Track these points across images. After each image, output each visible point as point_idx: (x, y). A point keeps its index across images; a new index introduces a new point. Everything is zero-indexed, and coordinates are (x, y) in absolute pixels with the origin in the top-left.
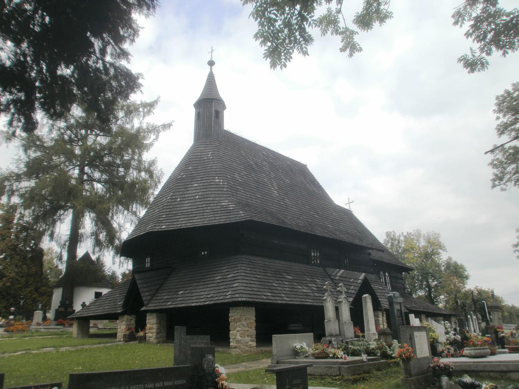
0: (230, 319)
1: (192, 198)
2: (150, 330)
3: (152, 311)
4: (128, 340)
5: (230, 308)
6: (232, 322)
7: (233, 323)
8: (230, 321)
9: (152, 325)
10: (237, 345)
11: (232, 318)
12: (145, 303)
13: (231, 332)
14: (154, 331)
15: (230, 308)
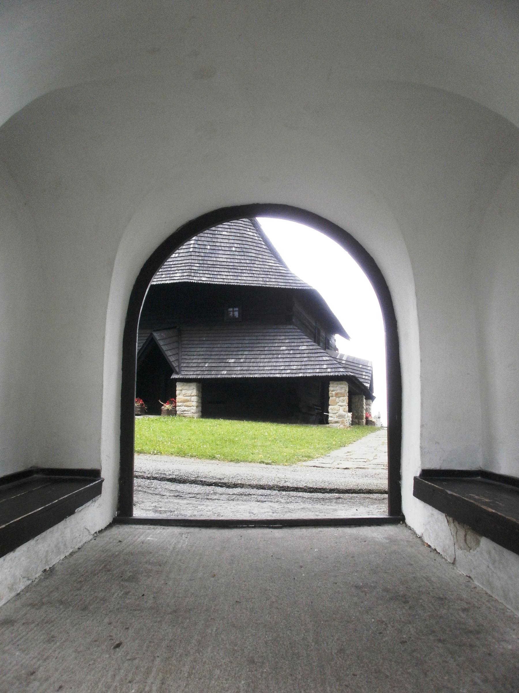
0: (331, 393)
1: (227, 249)
2: (184, 402)
3: (187, 381)
4: (139, 413)
5: (330, 382)
6: (332, 396)
7: (335, 397)
8: (330, 395)
9: (188, 398)
10: (339, 420)
11: (334, 393)
12: (177, 369)
13: (330, 407)
14: (195, 404)
15: (330, 382)
